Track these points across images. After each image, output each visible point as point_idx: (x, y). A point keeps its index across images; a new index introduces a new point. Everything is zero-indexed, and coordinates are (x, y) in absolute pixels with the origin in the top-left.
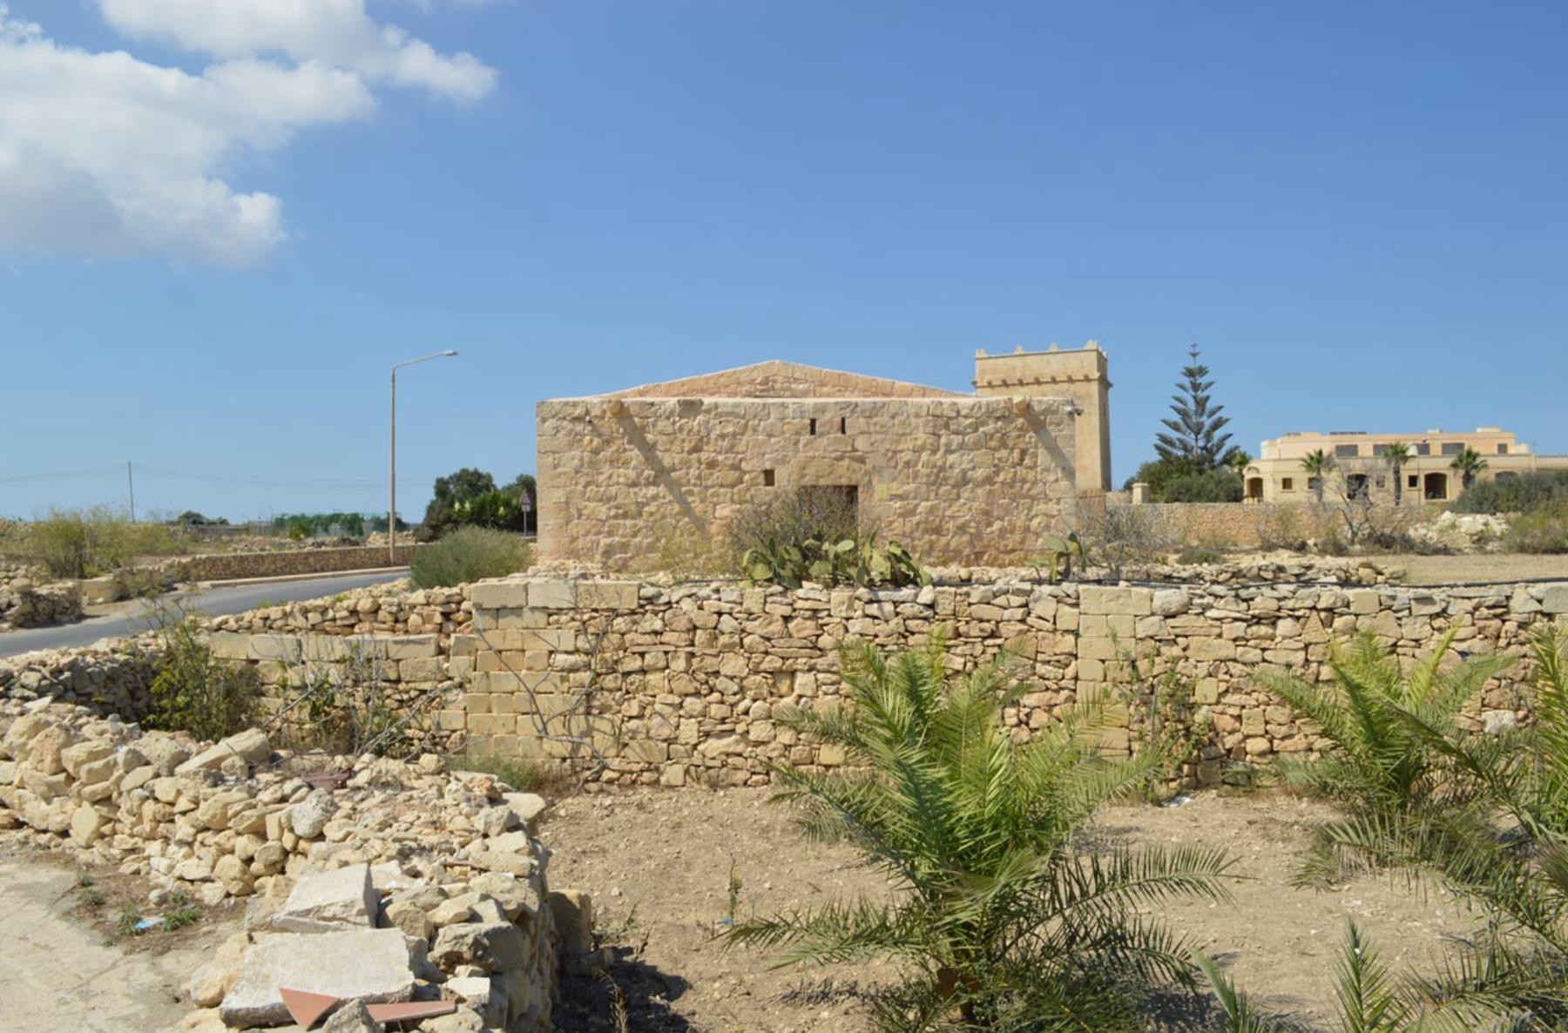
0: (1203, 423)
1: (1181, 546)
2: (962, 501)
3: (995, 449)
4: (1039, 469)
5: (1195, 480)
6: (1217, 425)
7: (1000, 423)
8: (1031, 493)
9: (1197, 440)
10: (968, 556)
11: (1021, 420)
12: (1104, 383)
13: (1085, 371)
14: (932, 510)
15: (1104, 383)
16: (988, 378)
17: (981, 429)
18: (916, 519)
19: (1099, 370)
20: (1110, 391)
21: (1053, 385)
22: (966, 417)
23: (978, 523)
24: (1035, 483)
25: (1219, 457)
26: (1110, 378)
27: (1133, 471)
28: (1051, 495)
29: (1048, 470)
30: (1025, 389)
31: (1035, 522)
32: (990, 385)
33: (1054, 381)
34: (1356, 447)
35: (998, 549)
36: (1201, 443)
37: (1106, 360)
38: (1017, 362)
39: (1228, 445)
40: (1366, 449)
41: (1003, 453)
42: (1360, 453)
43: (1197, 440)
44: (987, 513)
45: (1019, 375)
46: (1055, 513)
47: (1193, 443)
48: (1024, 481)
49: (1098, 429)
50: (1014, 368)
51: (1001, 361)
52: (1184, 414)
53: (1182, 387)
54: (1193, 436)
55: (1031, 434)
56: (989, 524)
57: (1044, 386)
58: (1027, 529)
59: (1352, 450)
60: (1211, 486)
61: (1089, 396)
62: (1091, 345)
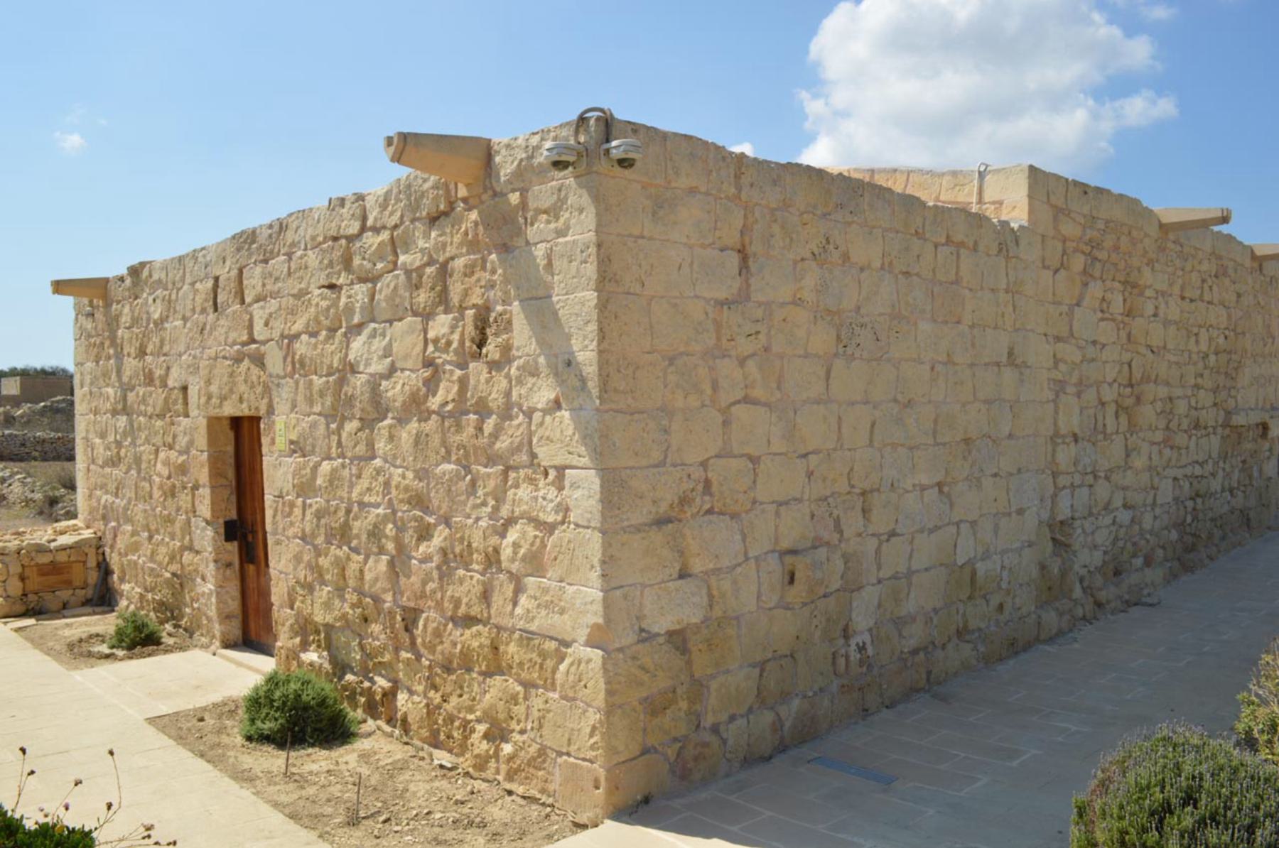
2: (378, 462)
3: (427, 316)
4: (513, 371)
7: (433, 234)
8: (502, 444)
10: (391, 613)
11: (474, 215)
14: (333, 477)
17: (402, 258)
18: (317, 502)
22: (376, 230)
23: (400, 529)
24: (506, 415)
28: (546, 455)
29: (535, 373)
31: (512, 535)
35: (439, 605)
41: (441, 325)
44: (419, 501)
46: (550, 519)
48: (482, 410)
55: (493, 256)
56: (424, 534)
58: (492, 559)
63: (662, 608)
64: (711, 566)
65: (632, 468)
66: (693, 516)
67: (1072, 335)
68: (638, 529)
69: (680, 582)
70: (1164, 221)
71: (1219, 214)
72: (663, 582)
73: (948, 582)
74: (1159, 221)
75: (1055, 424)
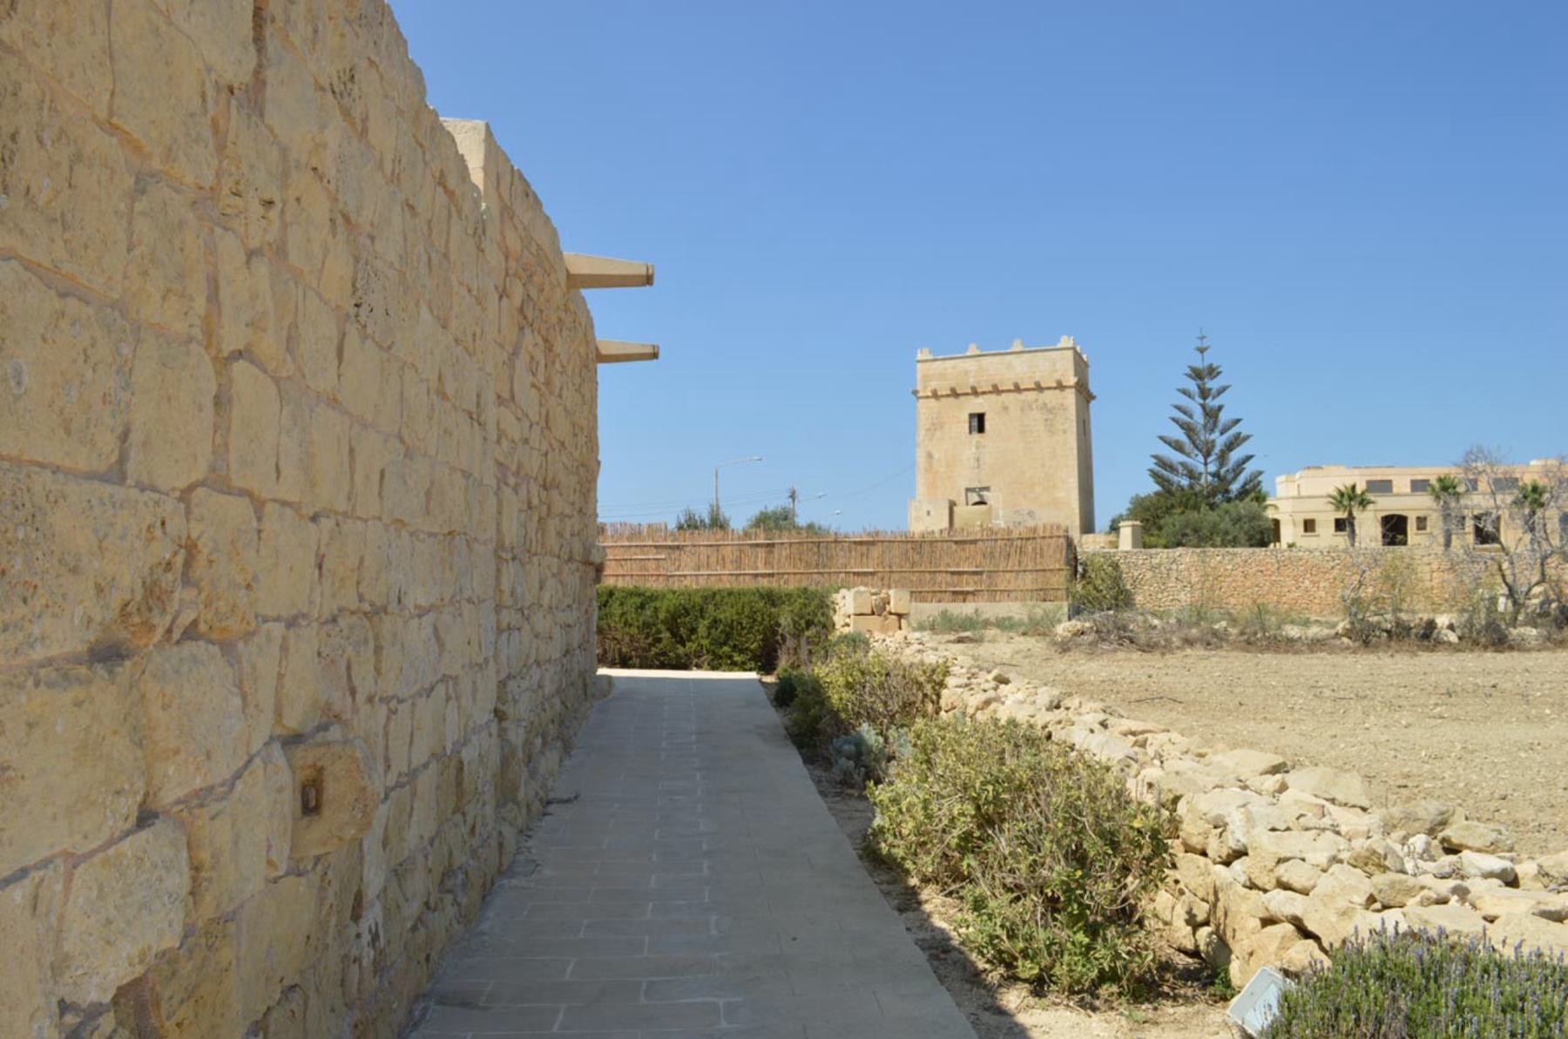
0: (1213, 441)
1: (1194, 632)
5: (1206, 517)
6: (1230, 446)
9: (1206, 464)
12: (1084, 394)
13: (1057, 376)
15: (1084, 394)
16: (933, 385)
19: (1075, 375)
20: (1093, 404)
21: (1015, 394)
25: (1235, 487)
26: (1093, 388)
27: (1123, 507)
30: (980, 399)
32: (935, 395)
33: (1017, 389)
34: (1390, 482)
36: (1212, 468)
37: (1086, 365)
38: (970, 365)
39: (1250, 468)
40: (1402, 484)
42: (1395, 490)
43: (1206, 464)
45: (972, 381)
47: (1201, 468)
49: (1075, 452)
50: (966, 373)
51: (949, 364)
52: (1189, 429)
53: (1185, 392)
54: (1201, 458)
57: (1004, 395)
59: (1384, 487)
60: (1226, 524)
61: (1063, 408)
62: (1066, 341)
63: (109, 922)
64: (198, 782)
65: (56, 470)
66: (158, 646)
67: (513, 397)
68: (62, 673)
69: (144, 834)
70: (573, 271)
71: (643, 271)
72: (112, 842)
73: (438, 788)
74: (567, 271)
75: (499, 531)
